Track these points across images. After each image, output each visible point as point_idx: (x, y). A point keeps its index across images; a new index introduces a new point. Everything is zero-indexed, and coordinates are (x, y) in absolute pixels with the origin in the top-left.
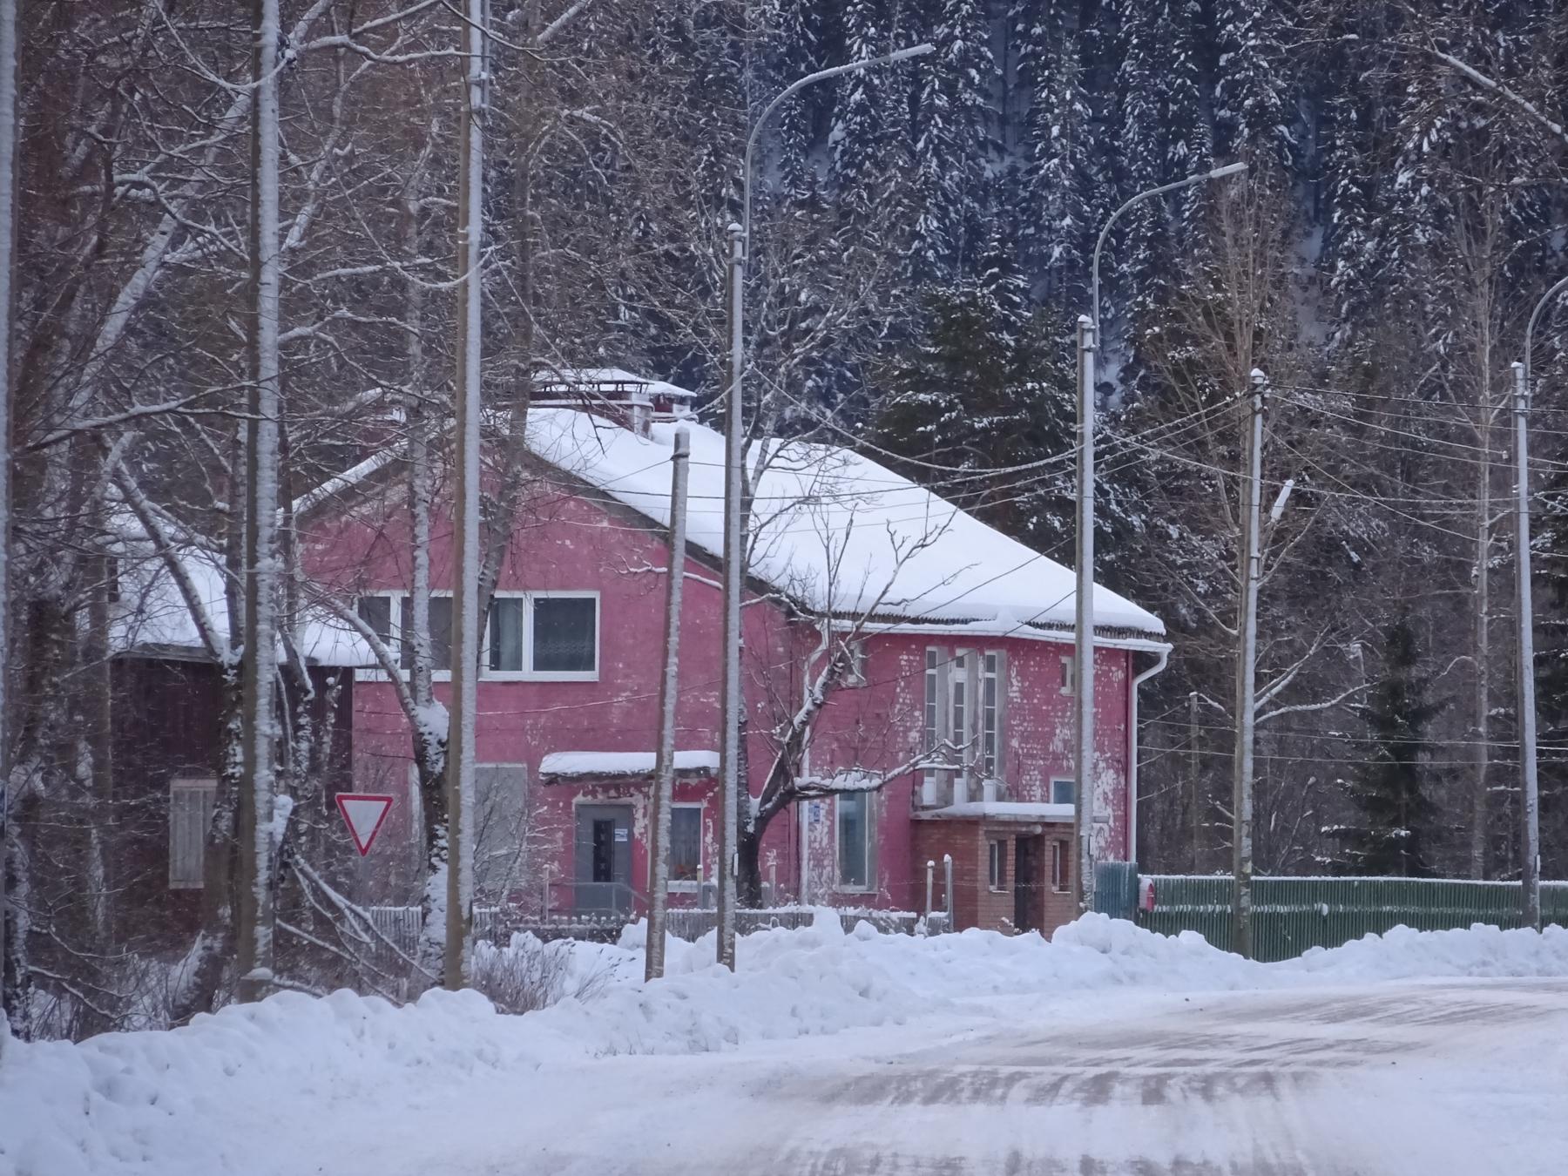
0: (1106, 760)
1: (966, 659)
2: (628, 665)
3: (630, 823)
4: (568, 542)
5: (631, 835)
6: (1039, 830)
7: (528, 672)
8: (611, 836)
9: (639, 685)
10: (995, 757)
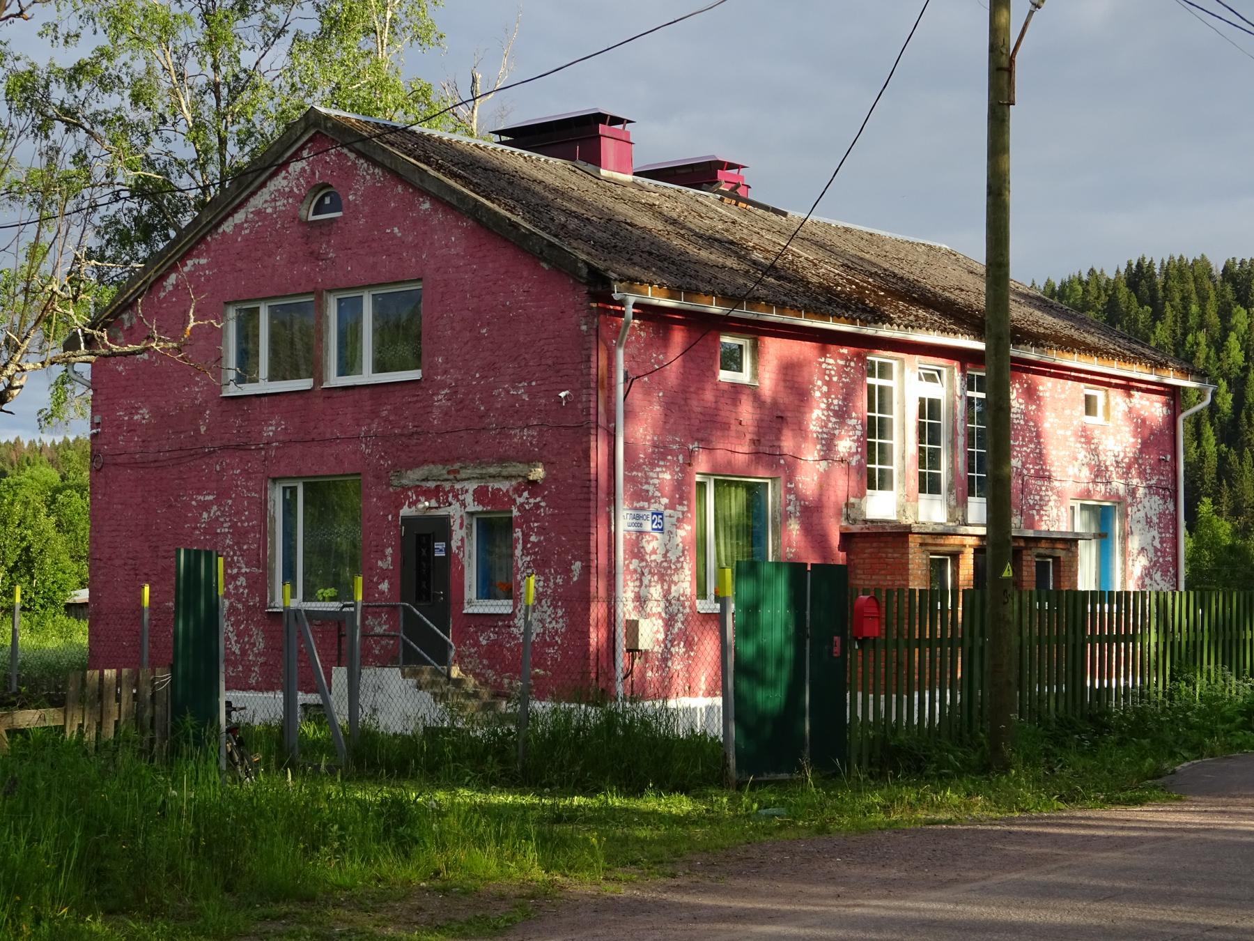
1: (945, 371)
2: (446, 361)
3: (446, 535)
4: (396, 230)
5: (448, 548)
7: (367, 376)
8: (431, 550)
9: (457, 380)
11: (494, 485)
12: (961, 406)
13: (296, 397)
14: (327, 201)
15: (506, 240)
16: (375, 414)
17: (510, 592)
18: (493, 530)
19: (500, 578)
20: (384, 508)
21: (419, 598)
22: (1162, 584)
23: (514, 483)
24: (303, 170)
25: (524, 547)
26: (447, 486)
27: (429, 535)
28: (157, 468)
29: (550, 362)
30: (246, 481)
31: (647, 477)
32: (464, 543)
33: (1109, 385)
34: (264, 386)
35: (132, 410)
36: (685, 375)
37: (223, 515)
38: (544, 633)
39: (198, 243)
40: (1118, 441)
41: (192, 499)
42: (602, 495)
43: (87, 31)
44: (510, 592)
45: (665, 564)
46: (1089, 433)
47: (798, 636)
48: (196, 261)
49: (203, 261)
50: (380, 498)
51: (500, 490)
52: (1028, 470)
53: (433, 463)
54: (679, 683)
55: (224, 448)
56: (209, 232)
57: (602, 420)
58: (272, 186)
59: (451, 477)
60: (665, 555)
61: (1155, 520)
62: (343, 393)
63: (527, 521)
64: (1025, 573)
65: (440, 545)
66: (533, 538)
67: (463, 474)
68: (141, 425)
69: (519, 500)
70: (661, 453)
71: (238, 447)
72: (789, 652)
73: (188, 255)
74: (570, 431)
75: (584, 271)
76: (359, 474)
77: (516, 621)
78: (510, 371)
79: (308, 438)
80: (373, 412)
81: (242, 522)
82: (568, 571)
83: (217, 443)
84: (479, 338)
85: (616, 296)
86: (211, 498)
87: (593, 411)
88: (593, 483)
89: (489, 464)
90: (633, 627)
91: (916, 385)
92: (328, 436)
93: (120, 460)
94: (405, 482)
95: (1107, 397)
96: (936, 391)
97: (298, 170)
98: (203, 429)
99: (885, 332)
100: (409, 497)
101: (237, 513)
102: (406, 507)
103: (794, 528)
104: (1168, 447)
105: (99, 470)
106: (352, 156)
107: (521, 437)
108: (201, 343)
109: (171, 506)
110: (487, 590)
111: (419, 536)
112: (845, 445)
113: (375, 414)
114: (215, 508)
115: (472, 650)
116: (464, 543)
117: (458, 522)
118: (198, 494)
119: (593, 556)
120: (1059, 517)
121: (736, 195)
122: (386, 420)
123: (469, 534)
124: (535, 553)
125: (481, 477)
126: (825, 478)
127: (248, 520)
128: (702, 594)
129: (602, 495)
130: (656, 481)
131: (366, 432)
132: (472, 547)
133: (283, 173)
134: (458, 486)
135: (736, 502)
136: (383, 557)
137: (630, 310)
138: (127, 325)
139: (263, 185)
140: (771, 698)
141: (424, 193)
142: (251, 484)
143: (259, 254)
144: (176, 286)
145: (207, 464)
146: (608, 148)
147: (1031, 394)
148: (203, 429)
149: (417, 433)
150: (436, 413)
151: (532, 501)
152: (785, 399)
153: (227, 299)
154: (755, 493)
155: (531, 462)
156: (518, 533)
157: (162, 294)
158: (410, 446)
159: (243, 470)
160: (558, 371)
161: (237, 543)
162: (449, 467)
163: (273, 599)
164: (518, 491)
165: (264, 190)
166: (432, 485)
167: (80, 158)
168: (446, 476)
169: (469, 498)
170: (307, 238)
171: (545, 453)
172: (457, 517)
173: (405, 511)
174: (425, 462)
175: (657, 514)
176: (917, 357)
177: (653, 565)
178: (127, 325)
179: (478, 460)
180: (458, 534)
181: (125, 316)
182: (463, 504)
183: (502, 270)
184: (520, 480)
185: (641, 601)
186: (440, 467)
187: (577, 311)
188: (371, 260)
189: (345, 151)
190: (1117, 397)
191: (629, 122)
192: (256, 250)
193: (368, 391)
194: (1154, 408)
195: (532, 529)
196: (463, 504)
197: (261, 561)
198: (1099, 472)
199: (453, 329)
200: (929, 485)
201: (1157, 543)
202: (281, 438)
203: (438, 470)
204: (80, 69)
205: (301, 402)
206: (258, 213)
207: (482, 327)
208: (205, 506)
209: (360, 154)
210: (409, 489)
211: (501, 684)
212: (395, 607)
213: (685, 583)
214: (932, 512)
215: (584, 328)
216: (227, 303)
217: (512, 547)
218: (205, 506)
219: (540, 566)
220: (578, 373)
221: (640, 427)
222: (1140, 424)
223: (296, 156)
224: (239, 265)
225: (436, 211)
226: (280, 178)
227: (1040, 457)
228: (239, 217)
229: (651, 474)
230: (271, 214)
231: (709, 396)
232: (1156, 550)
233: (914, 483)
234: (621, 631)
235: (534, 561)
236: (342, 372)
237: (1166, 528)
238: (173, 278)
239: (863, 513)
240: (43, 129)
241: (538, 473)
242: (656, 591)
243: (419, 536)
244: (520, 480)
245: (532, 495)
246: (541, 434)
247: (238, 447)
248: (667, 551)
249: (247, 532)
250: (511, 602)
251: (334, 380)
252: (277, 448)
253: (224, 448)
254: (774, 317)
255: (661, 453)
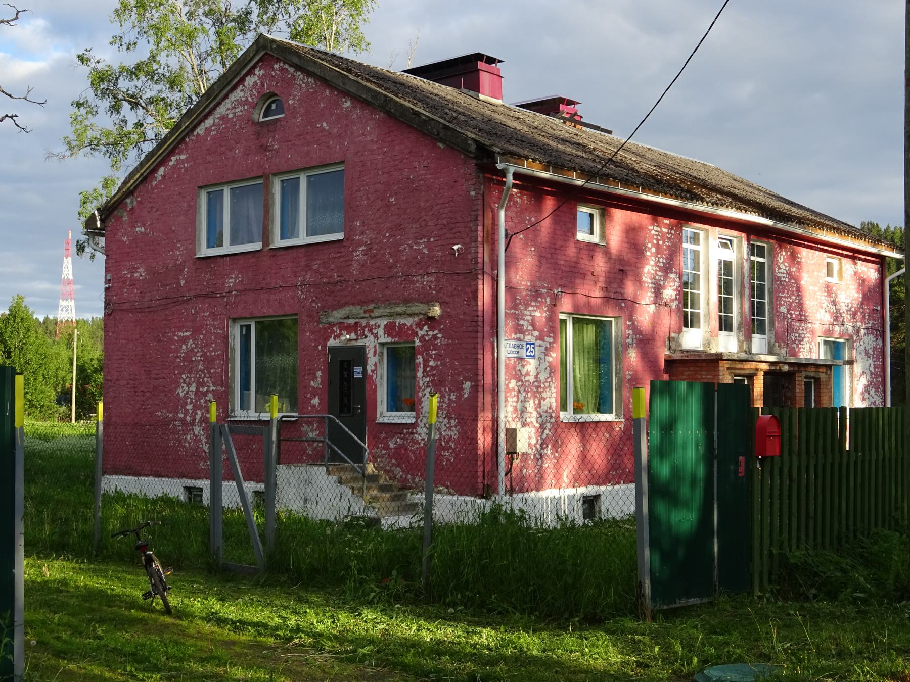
0: (867, 329)
1: (735, 241)
2: (363, 224)
3: (363, 362)
5: (364, 372)
6: (786, 368)
7: (303, 239)
8: (351, 373)
9: (371, 239)
10: (767, 319)
11: (400, 321)
12: (746, 266)
13: (250, 256)
14: (274, 106)
15: (410, 126)
16: (308, 267)
17: (413, 406)
18: (400, 358)
19: (405, 395)
20: (315, 340)
21: (342, 411)
22: (875, 397)
23: (416, 319)
24: (255, 83)
25: (424, 371)
26: (364, 322)
27: (349, 362)
28: (150, 312)
29: (445, 222)
30: (214, 320)
31: (523, 315)
32: (377, 368)
33: (842, 255)
34: (227, 248)
35: (133, 270)
36: (553, 235)
37: (196, 347)
38: (440, 439)
39: (179, 143)
40: (849, 295)
41: (175, 335)
42: (487, 328)
43: (142, 42)
44: (413, 406)
45: (536, 384)
46: (830, 291)
47: (709, 457)
48: (178, 157)
49: (183, 157)
50: (312, 332)
51: (405, 325)
52: (791, 315)
53: (353, 304)
54: (549, 478)
55: (198, 296)
56: (187, 134)
57: (487, 268)
58: (232, 97)
59: (367, 315)
60: (536, 377)
61: (871, 352)
62: (285, 252)
63: (427, 350)
64: (797, 390)
65: (358, 369)
66: (432, 363)
67: (377, 313)
68: (138, 280)
69: (421, 333)
70: (536, 294)
71: (207, 296)
72: (701, 471)
73: (172, 152)
74: (461, 277)
75: (473, 147)
76: (296, 314)
77: (419, 430)
78: (413, 230)
79: (258, 287)
80: (307, 266)
81: (211, 352)
82: (460, 389)
83: (192, 293)
84: (388, 206)
85: (500, 166)
86: (188, 334)
87: (480, 260)
88: (480, 319)
89: (397, 305)
90: (512, 434)
91: (713, 252)
92: (273, 285)
93: (125, 307)
94: (331, 319)
95: (841, 264)
96: (730, 255)
97: (251, 84)
98: (182, 282)
99: (699, 207)
100: (334, 332)
101: (206, 346)
102: (332, 340)
103: (633, 356)
104: (878, 301)
105: (110, 315)
106: (291, 70)
107: (422, 283)
108: (182, 218)
109: (160, 341)
110: (395, 404)
111: (342, 362)
112: (669, 293)
113: (308, 267)
114: (191, 341)
115: (384, 452)
116: (377, 368)
117: (373, 350)
118: (179, 331)
119: (480, 378)
120: (812, 350)
121: (574, 119)
122: (317, 272)
123: (381, 361)
124: (433, 375)
125: (390, 315)
126: (656, 316)
127: (215, 350)
128: (564, 407)
129: (487, 328)
130: (529, 318)
131: (302, 282)
132: (383, 371)
133: (241, 87)
134: (372, 322)
135: (589, 334)
136: (314, 378)
137: (510, 179)
138: (130, 207)
139: (226, 97)
140: (683, 519)
141: (346, 94)
142: (216, 323)
143: (223, 149)
144: (164, 177)
145: (185, 309)
146: (485, 79)
147: (793, 257)
148: (182, 282)
149: (340, 281)
150: (355, 265)
151: (431, 333)
152: (628, 256)
153: (200, 184)
154: (602, 327)
155: (429, 302)
156: (420, 359)
157: (154, 183)
158: (334, 294)
159: (212, 314)
160: (452, 229)
161: (207, 368)
162: (365, 308)
163: (233, 410)
164: (420, 325)
165: (227, 101)
166: (352, 321)
167: (139, 125)
168: (363, 315)
169: (381, 332)
170: (258, 135)
171: (441, 295)
172: (371, 346)
173: (331, 343)
174: (346, 304)
175: (530, 344)
176: (718, 229)
177: (527, 384)
178: (130, 207)
179: (388, 301)
180: (372, 360)
181: (128, 200)
182: (376, 337)
183: (406, 151)
184: (421, 317)
185: (522, 412)
186: (359, 307)
187: (467, 180)
188: (306, 148)
189: (286, 66)
190: (847, 264)
191: (500, 61)
192: (221, 146)
193: (303, 250)
194: (871, 272)
195: (431, 356)
196: (376, 337)
197: (224, 382)
198: (837, 317)
199: (368, 199)
200: (725, 325)
201: (872, 369)
202: (239, 288)
203: (357, 310)
204: (138, 67)
205: (253, 260)
206: (223, 118)
207: (391, 196)
208: (184, 340)
209: (298, 68)
210: (334, 325)
211: (406, 480)
212: (323, 418)
213: (551, 398)
214: (727, 344)
215: (473, 193)
216: (201, 187)
217: (415, 370)
218: (184, 340)
219: (437, 385)
220: (467, 230)
221: (519, 269)
222: (862, 282)
223: (250, 72)
224: (209, 158)
225: (354, 107)
226: (238, 91)
227: (801, 305)
228: (209, 122)
229: (526, 312)
230: (232, 119)
231: (571, 251)
232: (872, 374)
233: (715, 323)
234: (502, 436)
235: (432, 381)
236: (282, 238)
237: (878, 358)
238: (161, 171)
239: (680, 345)
240: (115, 108)
241: (437, 311)
242: (531, 406)
243: (342, 362)
244: (421, 317)
245: (431, 328)
246: (438, 280)
247: (207, 296)
248: (538, 373)
249: (214, 360)
250: (414, 413)
251: (278, 242)
252: (236, 295)
253: (198, 296)
254: (621, 191)
255: (536, 294)
